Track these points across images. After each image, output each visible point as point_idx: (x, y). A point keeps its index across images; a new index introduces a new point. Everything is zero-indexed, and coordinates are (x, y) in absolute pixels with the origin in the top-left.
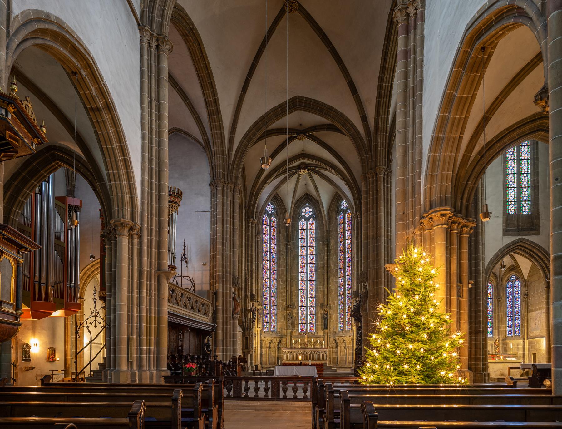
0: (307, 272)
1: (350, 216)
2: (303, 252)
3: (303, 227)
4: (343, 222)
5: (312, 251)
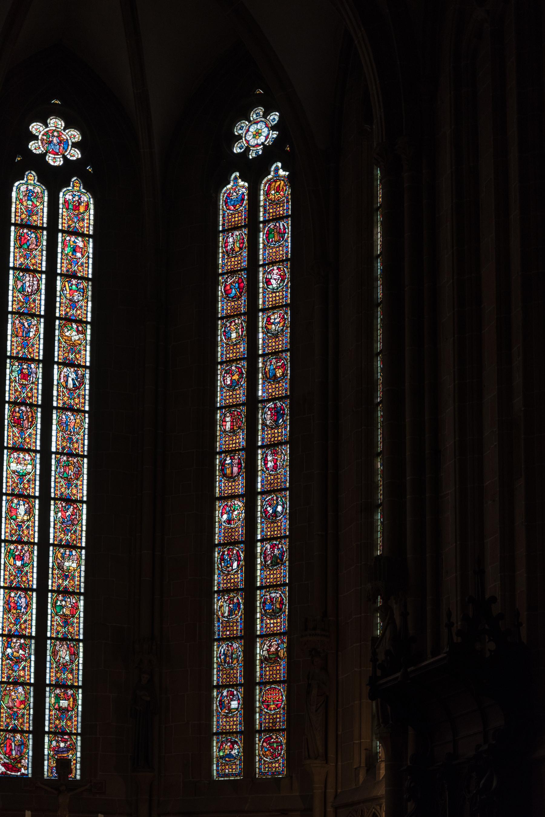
0: (45, 453)
2: (25, 343)
3: (31, 213)
5: (73, 347)
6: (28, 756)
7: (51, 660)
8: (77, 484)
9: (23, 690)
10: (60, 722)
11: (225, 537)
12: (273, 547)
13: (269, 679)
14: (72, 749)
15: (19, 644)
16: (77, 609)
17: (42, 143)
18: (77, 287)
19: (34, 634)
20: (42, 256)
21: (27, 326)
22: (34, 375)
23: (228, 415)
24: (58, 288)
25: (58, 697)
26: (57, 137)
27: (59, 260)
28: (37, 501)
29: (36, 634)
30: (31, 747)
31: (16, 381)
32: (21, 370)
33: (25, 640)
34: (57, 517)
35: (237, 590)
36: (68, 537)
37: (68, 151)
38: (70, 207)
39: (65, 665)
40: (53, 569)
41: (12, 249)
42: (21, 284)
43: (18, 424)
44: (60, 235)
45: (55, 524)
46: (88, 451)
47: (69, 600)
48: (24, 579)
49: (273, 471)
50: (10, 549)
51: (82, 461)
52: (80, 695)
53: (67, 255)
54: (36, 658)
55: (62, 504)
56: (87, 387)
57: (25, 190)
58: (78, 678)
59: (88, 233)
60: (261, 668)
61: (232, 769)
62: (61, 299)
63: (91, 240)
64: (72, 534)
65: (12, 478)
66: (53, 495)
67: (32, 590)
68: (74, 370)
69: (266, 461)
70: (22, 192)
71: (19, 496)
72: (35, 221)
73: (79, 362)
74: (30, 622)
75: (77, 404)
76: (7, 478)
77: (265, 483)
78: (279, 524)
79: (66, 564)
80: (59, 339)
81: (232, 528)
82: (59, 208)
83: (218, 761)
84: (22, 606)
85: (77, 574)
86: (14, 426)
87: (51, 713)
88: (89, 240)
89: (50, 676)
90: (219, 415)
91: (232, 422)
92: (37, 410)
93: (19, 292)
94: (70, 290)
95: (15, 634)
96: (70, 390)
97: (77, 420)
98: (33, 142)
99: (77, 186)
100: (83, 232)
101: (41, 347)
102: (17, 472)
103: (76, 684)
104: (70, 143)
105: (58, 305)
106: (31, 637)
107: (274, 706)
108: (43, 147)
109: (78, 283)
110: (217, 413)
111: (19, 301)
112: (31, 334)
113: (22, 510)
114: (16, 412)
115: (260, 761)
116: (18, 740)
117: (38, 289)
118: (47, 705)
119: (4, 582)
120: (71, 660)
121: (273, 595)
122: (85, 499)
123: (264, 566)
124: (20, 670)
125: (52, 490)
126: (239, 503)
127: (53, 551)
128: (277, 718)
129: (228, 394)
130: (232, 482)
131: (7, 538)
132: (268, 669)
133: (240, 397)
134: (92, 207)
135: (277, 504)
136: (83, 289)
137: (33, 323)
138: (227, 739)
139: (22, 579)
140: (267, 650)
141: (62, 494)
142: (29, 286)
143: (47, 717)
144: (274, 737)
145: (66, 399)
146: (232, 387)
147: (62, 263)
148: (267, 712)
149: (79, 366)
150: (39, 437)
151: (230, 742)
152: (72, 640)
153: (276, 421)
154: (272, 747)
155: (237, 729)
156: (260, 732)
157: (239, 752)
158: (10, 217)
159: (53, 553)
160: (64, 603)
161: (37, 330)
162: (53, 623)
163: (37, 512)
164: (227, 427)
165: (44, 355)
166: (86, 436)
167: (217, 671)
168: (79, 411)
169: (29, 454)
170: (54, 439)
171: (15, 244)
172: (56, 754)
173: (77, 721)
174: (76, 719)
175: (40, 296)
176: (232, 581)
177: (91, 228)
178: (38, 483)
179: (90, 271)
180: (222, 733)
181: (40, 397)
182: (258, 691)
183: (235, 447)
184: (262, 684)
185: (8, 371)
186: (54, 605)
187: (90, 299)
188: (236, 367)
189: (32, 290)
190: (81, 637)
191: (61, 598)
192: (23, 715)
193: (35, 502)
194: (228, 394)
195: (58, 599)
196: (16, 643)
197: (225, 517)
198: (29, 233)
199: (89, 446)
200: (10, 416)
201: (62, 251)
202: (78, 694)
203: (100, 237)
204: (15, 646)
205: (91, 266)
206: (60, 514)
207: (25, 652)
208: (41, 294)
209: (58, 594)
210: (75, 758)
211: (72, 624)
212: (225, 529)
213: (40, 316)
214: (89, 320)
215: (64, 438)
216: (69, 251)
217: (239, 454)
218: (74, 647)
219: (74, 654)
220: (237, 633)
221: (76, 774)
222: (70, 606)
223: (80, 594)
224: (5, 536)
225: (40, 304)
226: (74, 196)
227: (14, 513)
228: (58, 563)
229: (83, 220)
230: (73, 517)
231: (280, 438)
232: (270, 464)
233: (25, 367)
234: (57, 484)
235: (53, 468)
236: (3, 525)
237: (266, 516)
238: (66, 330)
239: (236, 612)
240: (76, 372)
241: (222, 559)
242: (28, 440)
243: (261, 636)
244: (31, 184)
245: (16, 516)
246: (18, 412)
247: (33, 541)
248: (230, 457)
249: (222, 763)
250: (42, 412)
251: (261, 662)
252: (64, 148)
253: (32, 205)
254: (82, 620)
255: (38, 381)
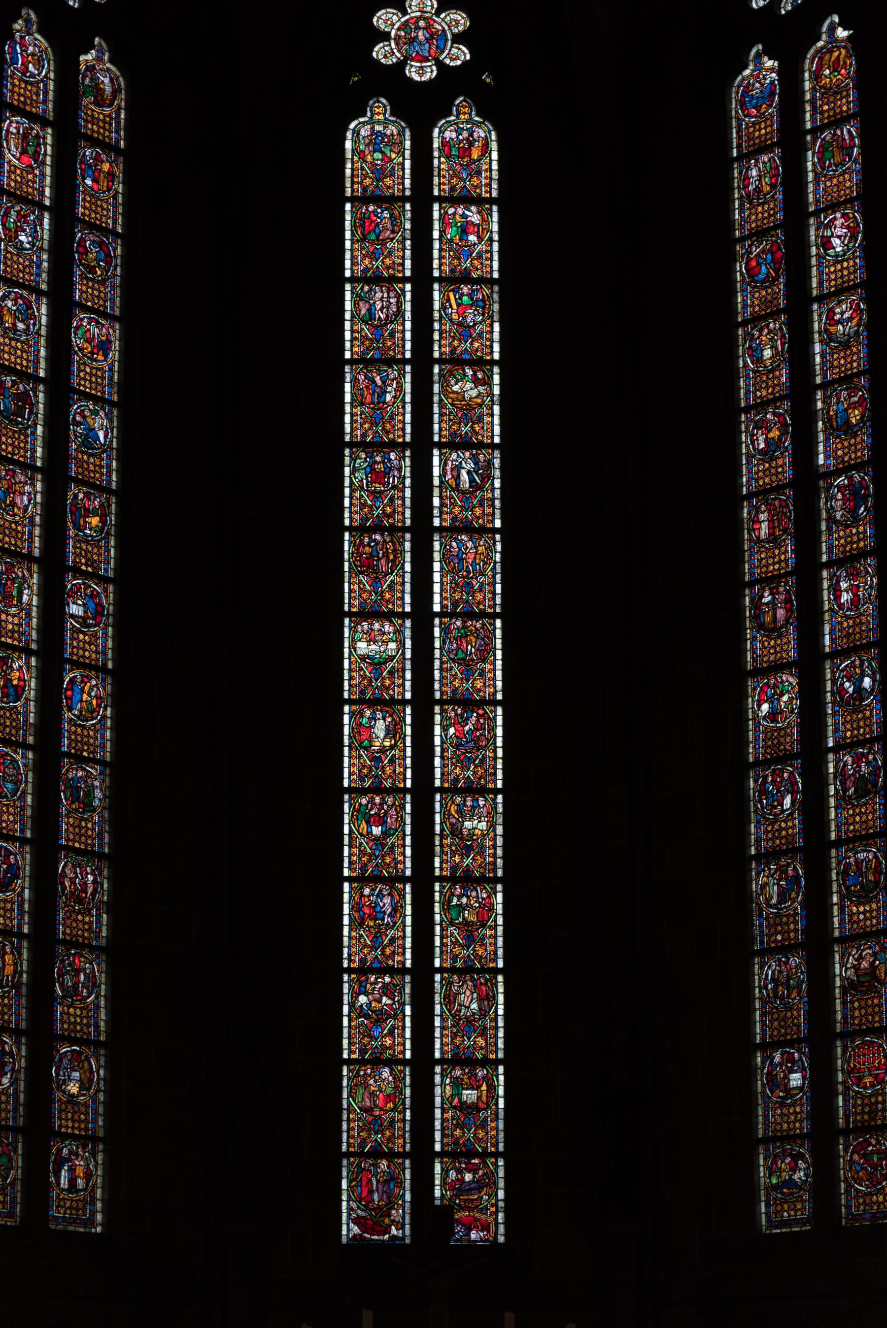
0: (422, 615)
1: (846, 75)
2: (378, 412)
3: (380, 174)
4: (769, 130)
5: (468, 411)
6: (404, 1201)
7: (442, 1012)
8: (483, 670)
9: (391, 1074)
10: (464, 1133)
11: (765, 747)
12: (857, 760)
13: (860, 1024)
14: (487, 1185)
15: (380, 985)
16: (490, 910)
17: (397, 44)
18: (472, 299)
19: (408, 964)
20: (404, 249)
21: (379, 383)
22: (396, 473)
23: (763, 508)
24: (437, 305)
25: (457, 1084)
26: (424, 28)
27: (436, 254)
28: (408, 710)
29: (412, 964)
30: (408, 1184)
31: (362, 488)
32: (372, 466)
33: (392, 977)
34: (446, 736)
35: (792, 851)
36: (470, 773)
37: (447, 52)
38: (454, 153)
39: (469, 1021)
40: (442, 836)
41: (348, 244)
42: (367, 306)
43: (368, 568)
44: (436, 207)
45: (443, 751)
46: (503, 605)
47: (474, 894)
48: (388, 860)
49: (851, 610)
50: (360, 804)
51: (491, 624)
52: (501, 1078)
53: (451, 241)
54: (412, 1011)
55: (455, 711)
56: (497, 483)
57: (369, 133)
58: (496, 1044)
59: (488, 195)
60: (844, 1003)
61: (796, 1211)
62: (441, 324)
63: (495, 208)
64: (476, 766)
65: (361, 669)
66: (437, 695)
67: (404, 880)
68: (471, 454)
69: (836, 591)
70: (364, 137)
71: (373, 703)
72: (389, 187)
73: (480, 437)
74: (401, 942)
75: (478, 518)
76: (350, 670)
77: (838, 634)
78: (868, 713)
79: (468, 824)
80: (441, 400)
81: (780, 729)
82: (433, 158)
83: (768, 1195)
84: (384, 913)
85: (488, 843)
86: (362, 573)
87: (446, 1115)
88: (491, 210)
89: (442, 1044)
90: (745, 510)
91: (771, 521)
92: (403, 538)
93: (363, 321)
94: (459, 305)
95: (374, 965)
96: (464, 492)
97: (480, 548)
98: (381, 45)
99: (464, 113)
100: (480, 194)
101: (408, 418)
102: (369, 657)
103: (493, 1056)
104: (449, 36)
105: (436, 336)
106: (403, 971)
107: (871, 1079)
108: (399, 51)
109: (473, 291)
110: (743, 508)
111: (365, 337)
112: (388, 397)
113: (380, 729)
114: (364, 546)
115: (847, 1191)
116: (384, 1172)
117: (400, 312)
118: (438, 1101)
119: (350, 868)
120: (480, 1009)
121: (861, 856)
122: (499, 696)
123: (843, 800)
124: (385, 1036)
125: (437, 686)
126: (791, 679)
127: (441, 802)
128: (877, 1102)
129: (761, 468)
130: (775, 639)
131: (353, 785)
132: (856, 1004)
133: (784, 472)
134: (494, 146)
135: (863, 675)
136: (483, 301)
137: (392, 376)
138: (784, 1151)
139: (383, 860)
140: (854, 966)
141: (455, 691)
142: (381, 309)
143: (438, 1124)
144: (873, 1142)
145: (457, 510)
146: (768, 454)
147: (441, 258)
148: (858, 1092)
149: (481, 445)
150: (408, 587)
151: (791, 1155)
152: (483, 970)
153: (853, 511)
154: (869, 1161)
155: (801, 1128)
156: (846, 1132)
157: (806, 1175)
158: (344, 187)
159: (441, 805)
160: (464, 900)
161: (400, 389)
162: (445, 941)
163: (408, 730)
164: (762, 533)
165: (412, 434)
166: (498, 577)
167: (761, 1015)
168: (483, 530)
169: (391, 622)
170: (437, 588)
171: (353, 235)
172: (457, 1196)
173: (497, 1128)
174: (494, 1124)
175: (403, 325)
176: (784, 833)
177: (495, 186)
178: (408, 675)
179: (496, 265)
180: (773, 1139)
181: (408, 513)
182: (839, 1050)
183: (779, 569)
184: (847, 1035)
185: (347, 470)
186: (446, 906)
187: (496, 318)
188: (774, 414)
189: (387, 315)
190: (501, 964)
191: (458, 891)
192: (392, 1122)
193: (404, 711)
194: (761, 468)
195: (452, 894)
196: (376, 983)
197: (765, 707)
198: (379, 210)
199: (503, 594)
200: (353, 553)
201: (441, 236)
202: (497, 1077)
203: (509, 201)
204: (373, 990)
205: (496, 257)
206: (452, 731)
207: (393, 999)
208: (404, 320)
209: (454, 885)
210: (493, 1201)
211: (482, 940)
212: (765, 732)
213: (404, 361)
214: (496, 356)
215: (457, 584)
216: (453, 234)
217: (786, 583)
218: (486, 984)
219: (487, 999)
220: (796, 937)
221: (496, 1234)
222: (477, 905)
223: (495, 880)
224: (350, 781)
225: (403, 339)
226: (459, 132)
227: (365, 735)
228: (452, 824)
229: (479, 173)
230: (478, 734)
231: (862, 544)
232: (845, 597)
233: (378, 459)
234: (444, 674)
235: (437, 644)
236: (346, 760)
237: (842, 699)
238: (453, 382)
239: (793, 895)
240: (475, 458)
241: (763, 791)
242: (387, 596)
243: (842, 940)
244: (379, 122)
245: (370, 742)
246: (369, 545)
247: (402, 785)
248: (770, 589)
249: (775, 1199)
250: (412, 541)
251: (844, 991)
252: (437, 47)
253: (382, 160)
254: (500, 929)
255: (404, 483)
